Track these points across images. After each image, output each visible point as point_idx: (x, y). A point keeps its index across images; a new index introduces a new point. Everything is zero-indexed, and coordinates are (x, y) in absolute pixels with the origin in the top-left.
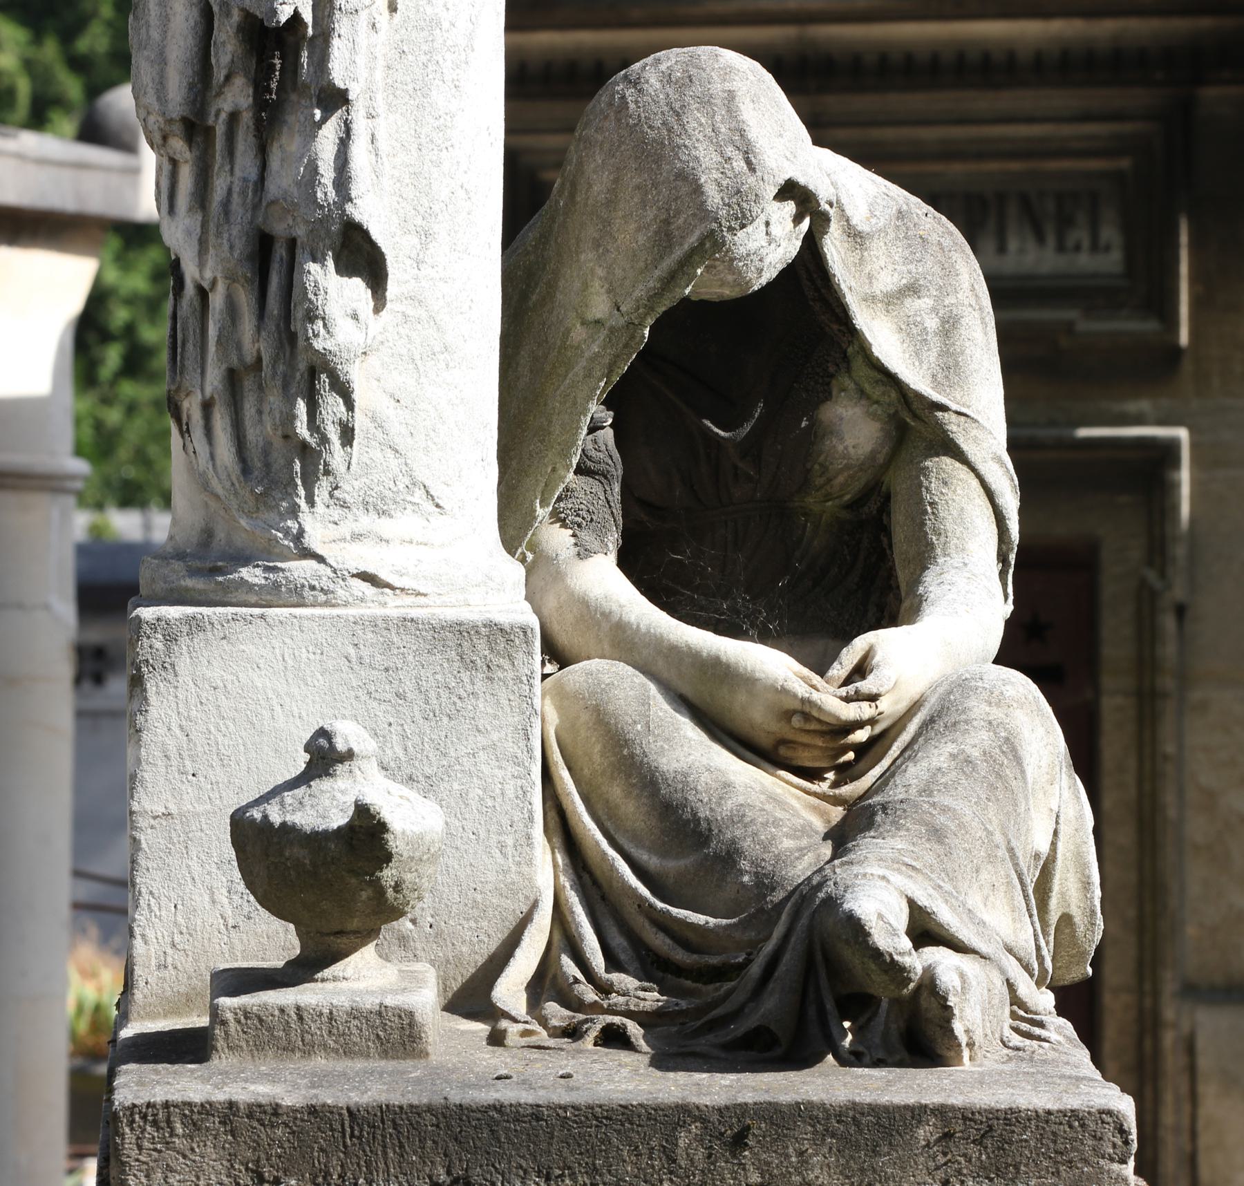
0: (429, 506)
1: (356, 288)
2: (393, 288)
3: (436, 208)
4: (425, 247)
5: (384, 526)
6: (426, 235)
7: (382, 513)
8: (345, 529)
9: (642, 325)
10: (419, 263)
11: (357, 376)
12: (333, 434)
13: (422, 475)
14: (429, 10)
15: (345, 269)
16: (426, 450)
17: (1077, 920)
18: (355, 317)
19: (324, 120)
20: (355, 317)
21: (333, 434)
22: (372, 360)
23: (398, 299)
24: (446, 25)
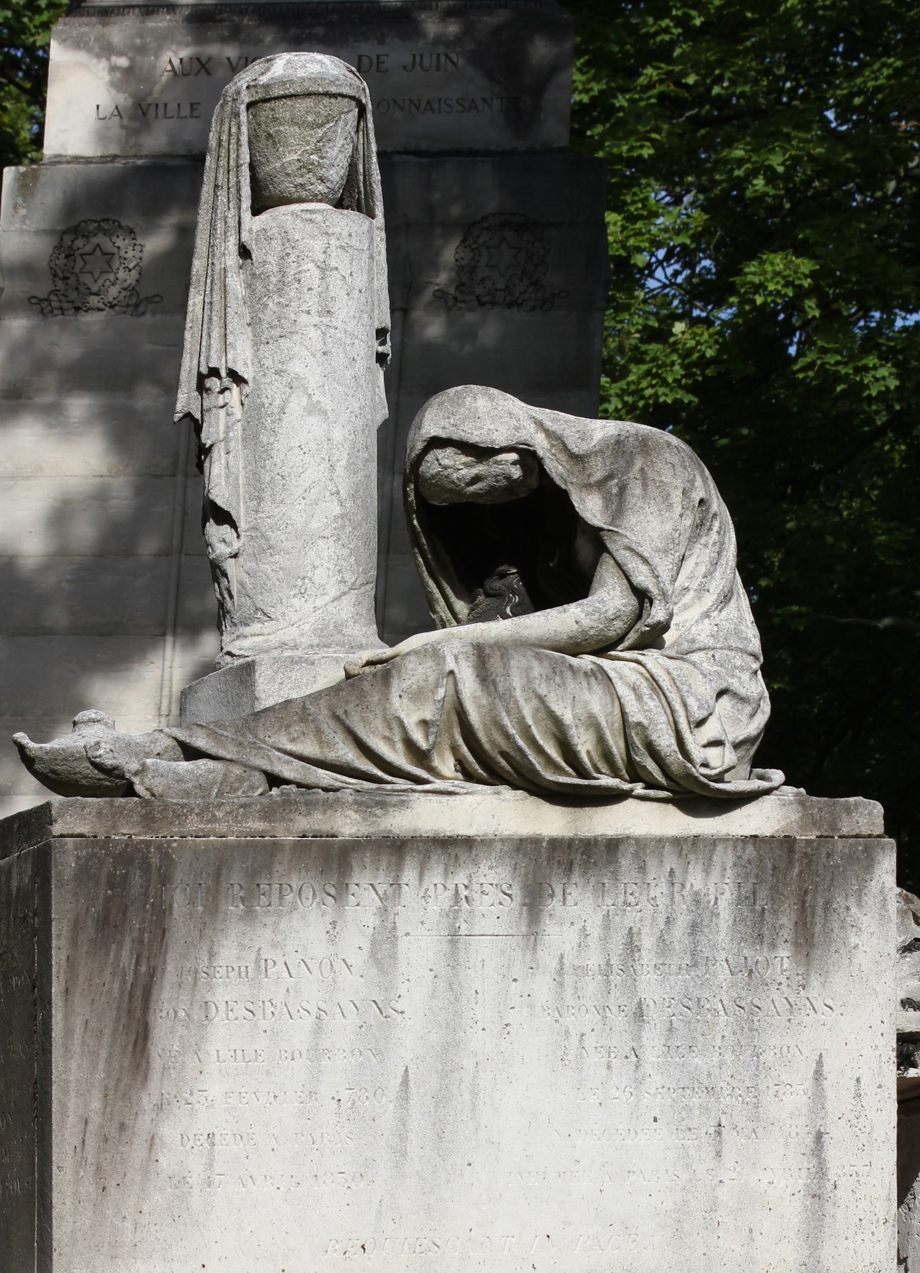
0: (266, 618)
1: (226, 530)
2: (242, 525)
3: (263, 486)
4: (259, 504)
5: (247, 630)
6: (260, 499)
7: (247, 625)
8: (234, 636)
9: (412, 521)
10: (257, 512)
11: (230, 566)
12: (226, 596)
13: (260, 605)
14: (259, 401)
15: (219, 522)
16: (261, 593)
17: (512, 753)
18: (224, 541)
19: (205, 458)
20: (224, 541)
21: (226, 596)
22: (241, 559)
23: (248, 530)
24: (267, 405)
